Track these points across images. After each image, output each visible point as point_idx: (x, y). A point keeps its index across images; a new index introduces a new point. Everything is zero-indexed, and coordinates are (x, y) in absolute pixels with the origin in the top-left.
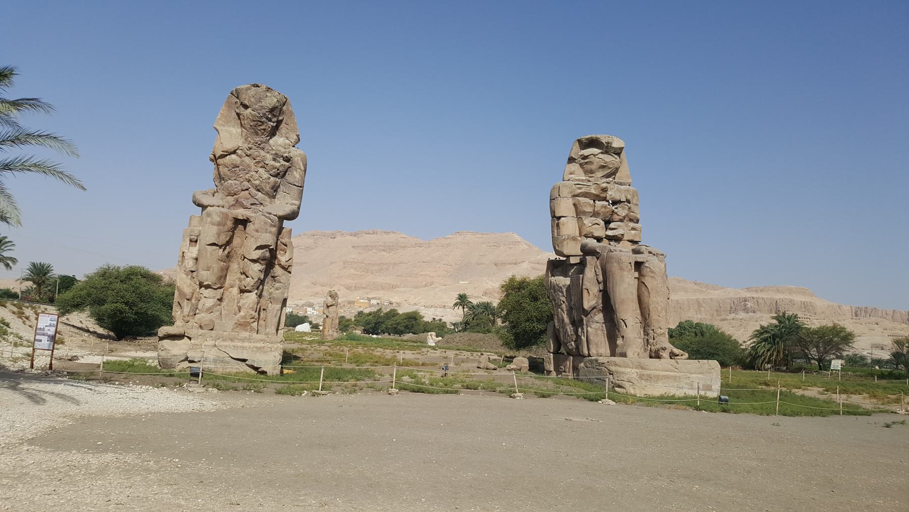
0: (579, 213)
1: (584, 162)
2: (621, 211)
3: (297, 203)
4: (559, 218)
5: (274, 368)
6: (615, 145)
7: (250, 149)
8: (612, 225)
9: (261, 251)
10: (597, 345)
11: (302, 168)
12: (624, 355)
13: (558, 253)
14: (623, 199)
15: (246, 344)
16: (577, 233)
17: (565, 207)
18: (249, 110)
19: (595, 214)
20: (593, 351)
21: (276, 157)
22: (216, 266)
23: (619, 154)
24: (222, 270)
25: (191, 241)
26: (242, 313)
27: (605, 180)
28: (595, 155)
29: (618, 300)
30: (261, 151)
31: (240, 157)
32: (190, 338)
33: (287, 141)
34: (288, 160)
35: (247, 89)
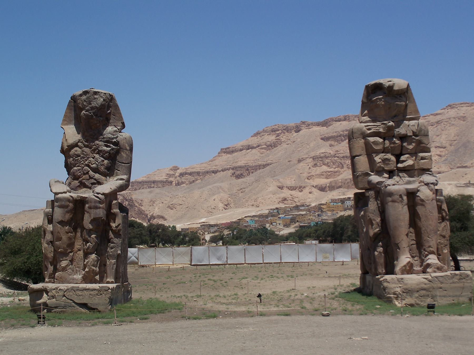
3: (125, 177)
6: (396, 88)
8: (403, 158)
11: (128, 148)
13: (357, 187)
14: (410, 134)
18: (84, 112)
20: (380, 271)
24: (70, 238)
26: (87, 270)
28: (380, 99)
31: (80, 148)
32: (47, 293)
33: (115, 129)
34: (116, 144)
35: (81, 95)
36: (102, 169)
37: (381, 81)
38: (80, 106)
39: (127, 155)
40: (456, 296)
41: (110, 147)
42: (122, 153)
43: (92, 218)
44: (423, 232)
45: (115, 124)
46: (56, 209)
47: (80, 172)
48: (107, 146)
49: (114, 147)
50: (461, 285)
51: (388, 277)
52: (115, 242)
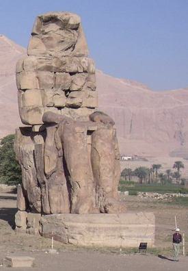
0: (42, 86)
1: (47, 39)
2: (79, 81)
4: (24, 90)
6: (71, 22)
10: (57, 204)
12: (77, 212)
13: (24, 123)
16: (41, 104)
17: (29, 81)
19: (54, 87)
20: (54, 210)
23: (76, 29)
27: (64, 54)
28: (54, 32)
29: (73, 166)
37: (56, 14)
40: (141, 237)
44: (101, 171)
50: (145, 226)
51: (71, 216)
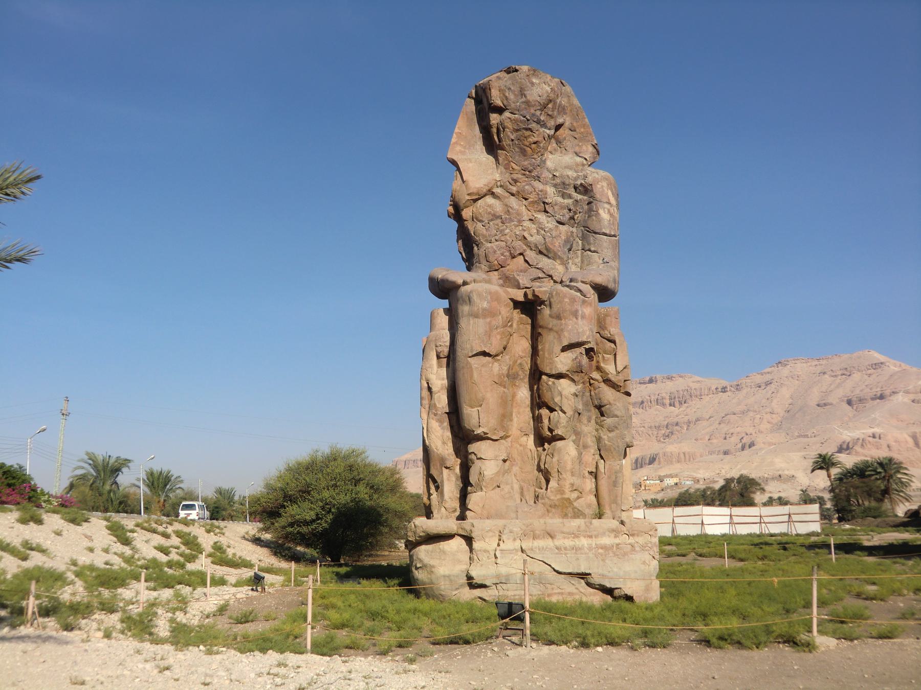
5: (648, 589)
7: (516, 181)
9: (570, 355)
11: (613, 201)
15: (584, 542)
18: (507, 114)
21: (562, 187)
22: (492, 396)
25: (438, 357)
26: (553, 484)
30: (537, 184)
32: (469, 540)
33: (578, 159)
34: (585, 189)
36: (557, 245)
38: (499, 102)
39: (611, 215)
41: (570, 197)
42: (601, 211)
43: (566, 343)
45: (577, 149)
46: (463, 323)
47: (502, 254)
48: (563, 196)
49: (579, 197)
52: (618, 413)
